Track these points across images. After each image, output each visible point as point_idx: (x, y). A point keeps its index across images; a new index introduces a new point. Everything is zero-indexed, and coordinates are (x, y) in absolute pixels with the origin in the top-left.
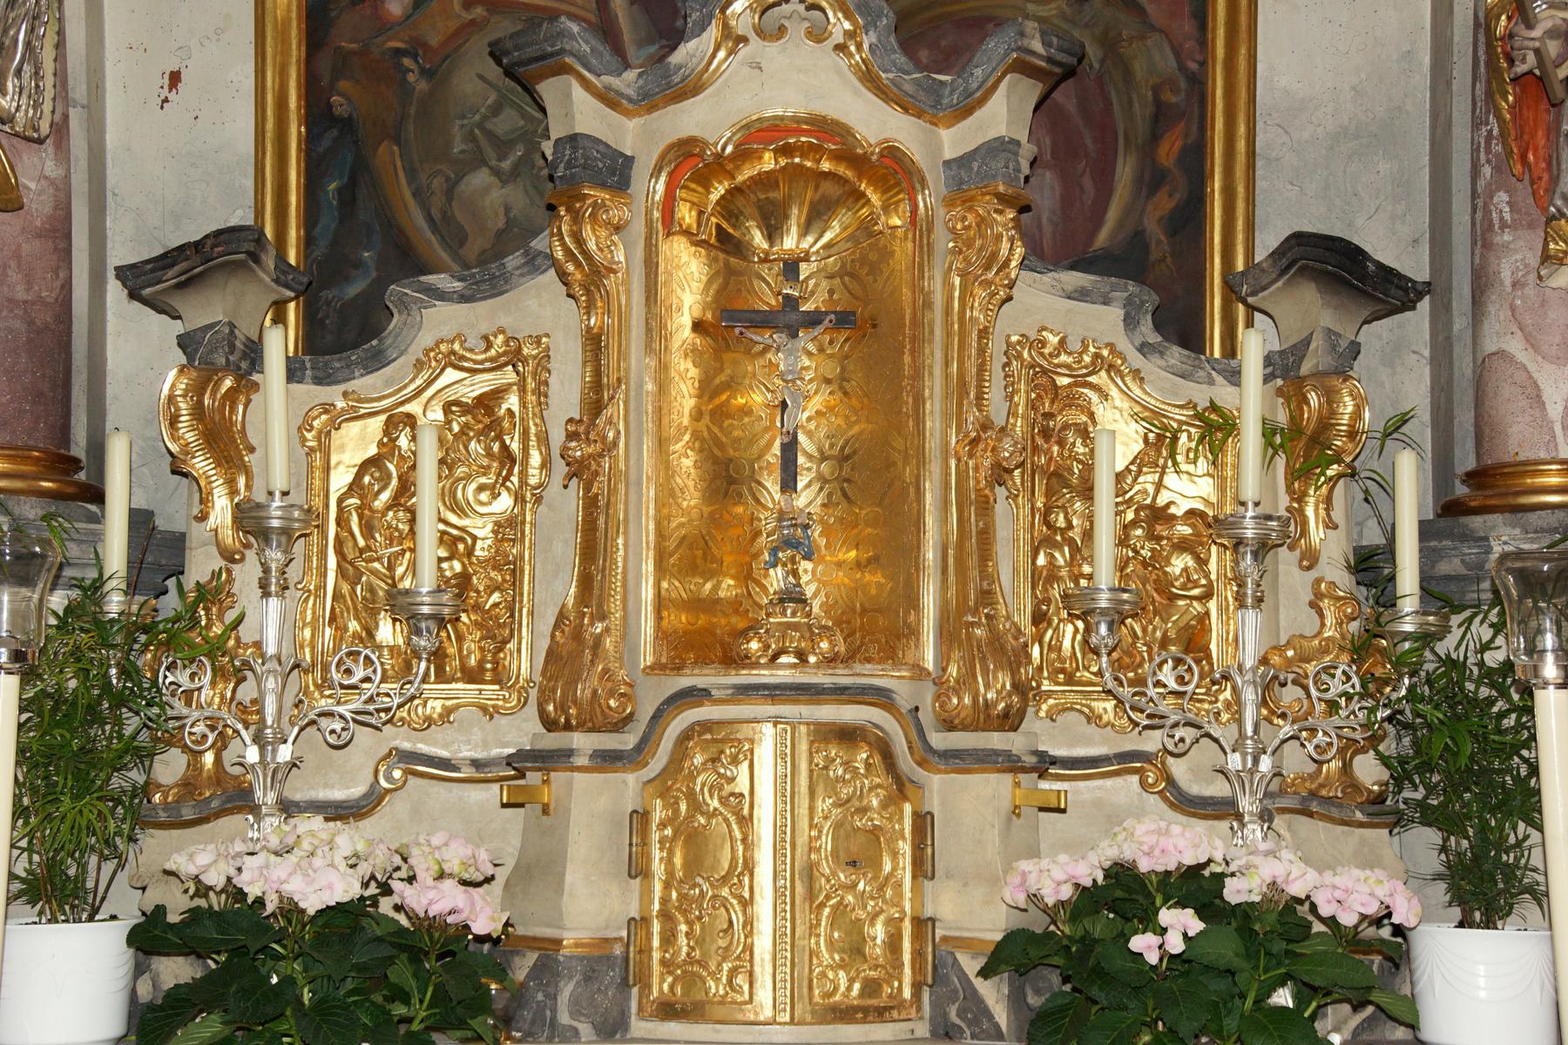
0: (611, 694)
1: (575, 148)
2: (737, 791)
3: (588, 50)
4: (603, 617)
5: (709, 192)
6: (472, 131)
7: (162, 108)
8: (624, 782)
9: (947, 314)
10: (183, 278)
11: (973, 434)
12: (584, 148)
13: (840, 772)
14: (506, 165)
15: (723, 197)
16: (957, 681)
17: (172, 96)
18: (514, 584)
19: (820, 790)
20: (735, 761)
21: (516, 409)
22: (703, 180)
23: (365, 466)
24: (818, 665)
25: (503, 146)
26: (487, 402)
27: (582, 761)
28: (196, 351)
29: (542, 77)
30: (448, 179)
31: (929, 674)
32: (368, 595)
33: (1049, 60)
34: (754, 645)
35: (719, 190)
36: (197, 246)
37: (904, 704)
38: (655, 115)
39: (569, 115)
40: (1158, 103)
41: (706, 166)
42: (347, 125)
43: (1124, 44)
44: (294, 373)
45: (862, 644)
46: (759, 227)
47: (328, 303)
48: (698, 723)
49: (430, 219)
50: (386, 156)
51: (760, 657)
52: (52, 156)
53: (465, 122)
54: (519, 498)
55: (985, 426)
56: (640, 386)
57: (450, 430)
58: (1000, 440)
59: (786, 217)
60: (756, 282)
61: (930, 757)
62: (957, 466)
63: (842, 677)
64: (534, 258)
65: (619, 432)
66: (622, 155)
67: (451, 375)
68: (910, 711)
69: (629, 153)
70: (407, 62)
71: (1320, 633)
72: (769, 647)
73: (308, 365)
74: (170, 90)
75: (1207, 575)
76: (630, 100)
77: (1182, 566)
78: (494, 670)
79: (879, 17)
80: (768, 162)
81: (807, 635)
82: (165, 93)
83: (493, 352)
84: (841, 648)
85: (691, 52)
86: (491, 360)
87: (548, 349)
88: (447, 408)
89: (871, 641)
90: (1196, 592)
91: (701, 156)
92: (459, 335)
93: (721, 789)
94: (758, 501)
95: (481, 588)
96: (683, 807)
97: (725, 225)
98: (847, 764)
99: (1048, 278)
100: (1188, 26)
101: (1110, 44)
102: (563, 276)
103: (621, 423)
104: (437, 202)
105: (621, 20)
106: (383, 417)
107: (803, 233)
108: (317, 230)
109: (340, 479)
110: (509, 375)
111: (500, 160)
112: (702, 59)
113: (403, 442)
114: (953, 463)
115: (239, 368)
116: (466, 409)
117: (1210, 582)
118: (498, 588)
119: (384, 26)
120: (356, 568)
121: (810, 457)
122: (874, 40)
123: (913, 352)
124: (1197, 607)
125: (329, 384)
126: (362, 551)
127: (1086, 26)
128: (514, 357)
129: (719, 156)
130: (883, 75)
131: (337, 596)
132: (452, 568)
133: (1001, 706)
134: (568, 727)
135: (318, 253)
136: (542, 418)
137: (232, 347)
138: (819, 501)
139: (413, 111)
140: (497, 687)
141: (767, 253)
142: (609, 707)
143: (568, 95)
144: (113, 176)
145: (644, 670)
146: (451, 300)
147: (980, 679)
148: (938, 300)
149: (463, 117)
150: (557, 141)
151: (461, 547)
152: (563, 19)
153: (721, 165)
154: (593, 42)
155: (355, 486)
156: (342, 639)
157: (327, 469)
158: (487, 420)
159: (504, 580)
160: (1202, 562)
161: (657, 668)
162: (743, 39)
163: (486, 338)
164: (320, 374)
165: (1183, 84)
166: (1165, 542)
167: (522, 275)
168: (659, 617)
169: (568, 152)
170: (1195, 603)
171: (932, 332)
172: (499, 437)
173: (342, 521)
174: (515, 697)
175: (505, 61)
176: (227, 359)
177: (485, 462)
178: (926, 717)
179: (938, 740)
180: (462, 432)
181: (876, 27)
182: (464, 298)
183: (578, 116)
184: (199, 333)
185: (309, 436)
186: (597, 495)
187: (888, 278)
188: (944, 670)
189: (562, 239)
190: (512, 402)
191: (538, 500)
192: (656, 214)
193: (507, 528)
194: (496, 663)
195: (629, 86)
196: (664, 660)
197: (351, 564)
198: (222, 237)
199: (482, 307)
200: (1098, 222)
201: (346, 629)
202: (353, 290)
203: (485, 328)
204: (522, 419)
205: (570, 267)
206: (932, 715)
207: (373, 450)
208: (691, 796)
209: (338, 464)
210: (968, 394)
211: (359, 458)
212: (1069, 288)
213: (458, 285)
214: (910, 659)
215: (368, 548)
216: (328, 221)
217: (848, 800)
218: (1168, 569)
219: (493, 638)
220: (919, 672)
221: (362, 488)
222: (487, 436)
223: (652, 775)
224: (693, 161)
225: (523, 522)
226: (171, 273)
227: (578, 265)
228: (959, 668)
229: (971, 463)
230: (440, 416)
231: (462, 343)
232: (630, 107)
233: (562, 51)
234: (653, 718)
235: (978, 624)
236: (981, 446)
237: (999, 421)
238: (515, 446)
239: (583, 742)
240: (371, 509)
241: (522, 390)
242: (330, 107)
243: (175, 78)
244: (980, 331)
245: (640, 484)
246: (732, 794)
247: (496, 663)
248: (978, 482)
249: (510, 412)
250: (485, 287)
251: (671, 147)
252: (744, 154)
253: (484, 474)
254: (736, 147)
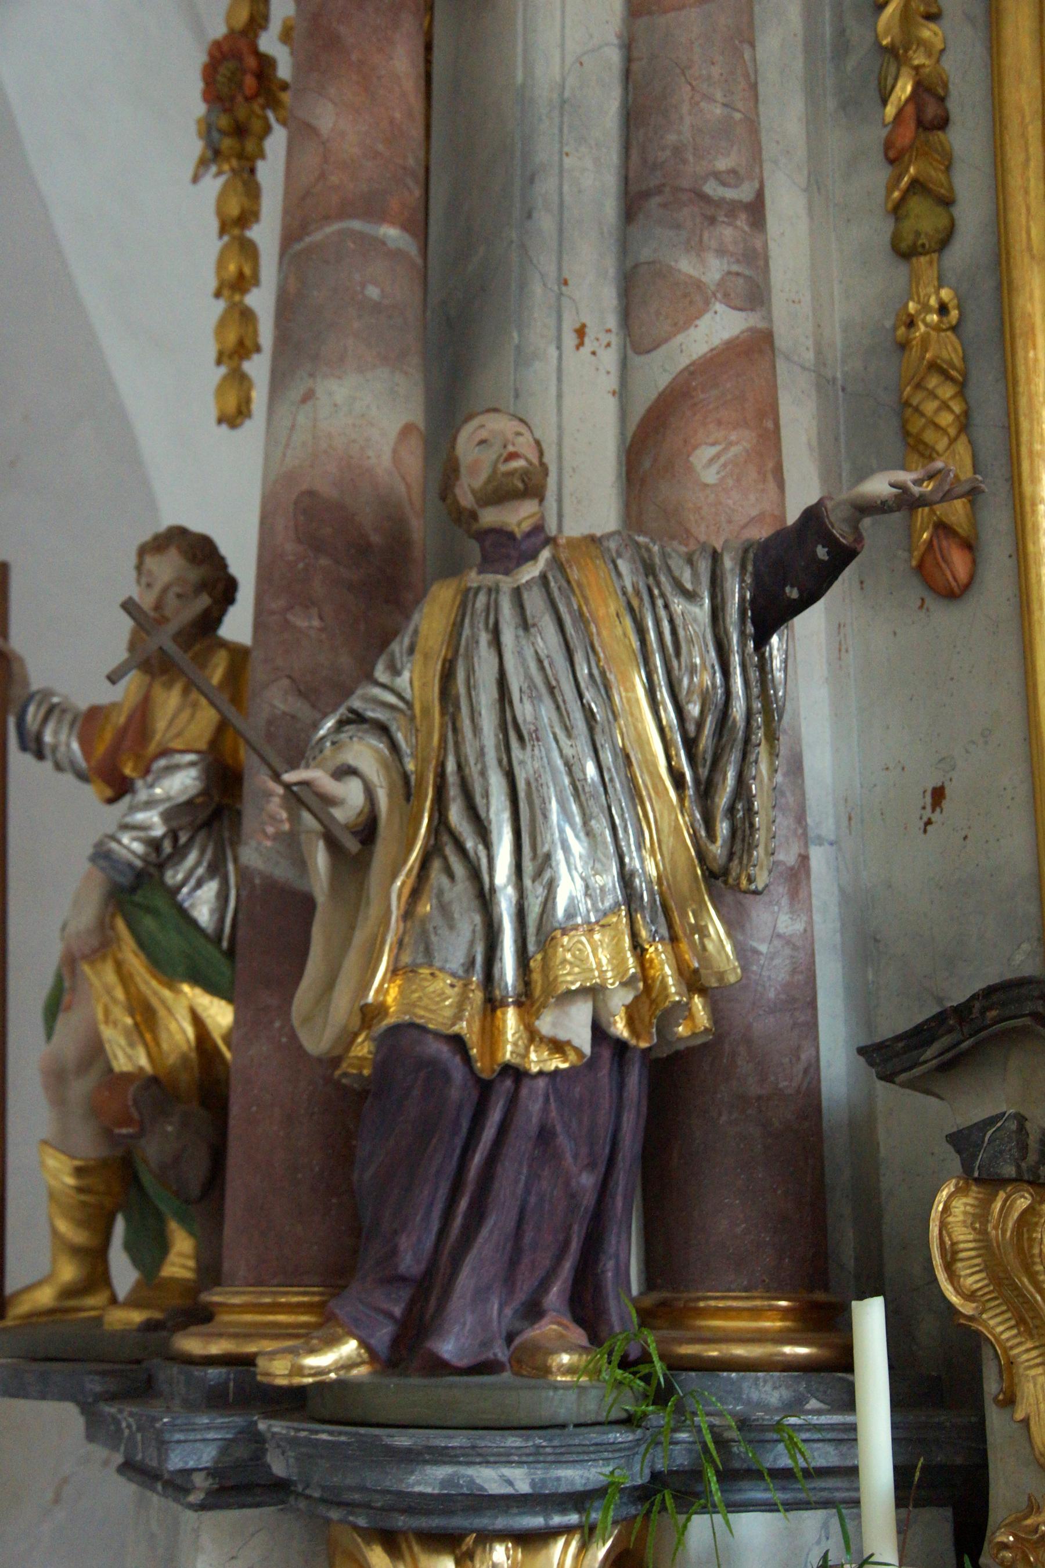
7: (925, 831)
10: (948, 1056)
17: (936, 817)
36: (962, 1012)
52: (786, 909)
74: (933, 811)
176: (1018, 1167)
198: (995, 998)
226: (929, 1053)
243: (938, 795)
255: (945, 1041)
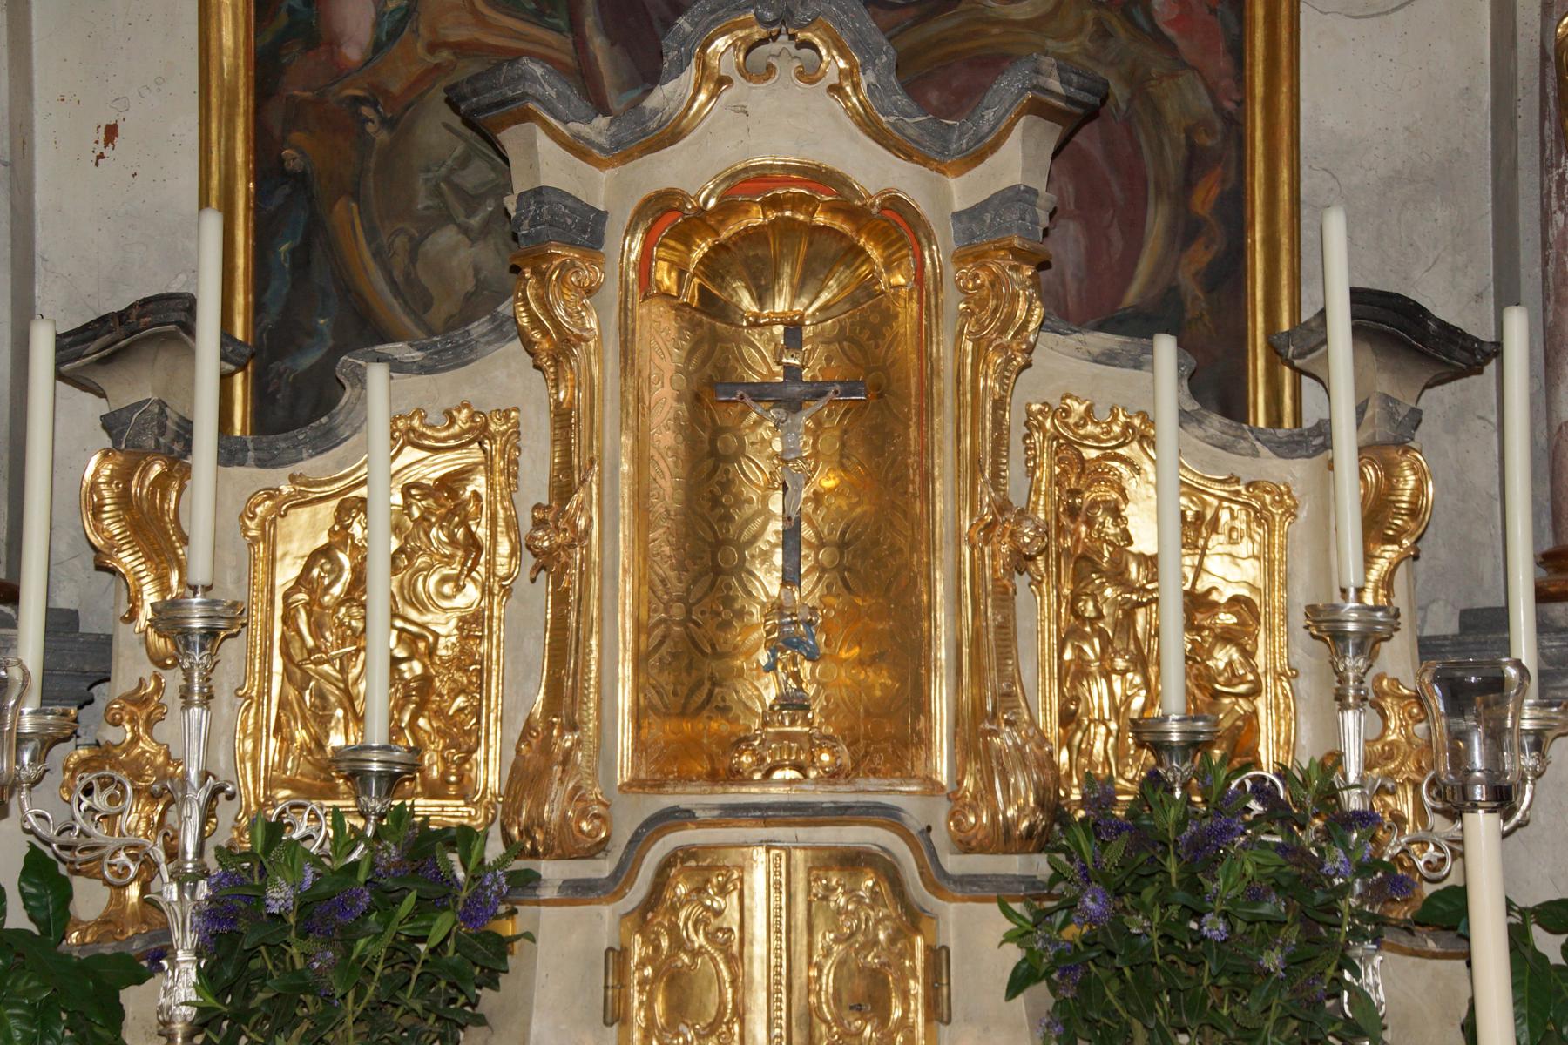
0: (583, 814)
1: (540, 203)
2: (725, 925)
3: (553, 94)
4: (573, 727)
5: (691, 251)
6: (437, 185)
7: (97, 164)
8: (599, 915)
9: (959, 382)
10: (106, 352)
11: (989, 518)
12: (550, 203)
13: (842, 902)
14: (475, 221)
15: (705, 255)
16: (974, 797)
17: (108, 152)
18: (480, 686)
19: (820, 922)
20: (723, 891)
21: (483, 491)
22: (684, 236)
23: (313, 558)
24: (817, 780)
25: (471, 201)
26: (450, 484)
27: (548, 893)
28: (122, 433)
29: (503, 125)
30: (411, 238)
31: (942, 788)
32: (318, 702)
33: (1069, 100)
34: (746, 759)
35: (701, 250)
36: (122, 316)
37: (915, 824)
38: (630, 165)
39: (533, 167)
40: (1191, 146)
41: (685, 221)
42: (301, 181)
43: (1153, 82)
44: (229, 453)
45: (867, 753)
46: (748, 288)
47: (280, 376)
48: (681, 848)
49: (392, 283)
50: (344, 214)
51: (752, 773)
53: (430, 175)
54: (486, 591)
55: (1003, 507)
56: (616, 466)
57: (410, 515)
58: (1018, 523)
59: (777, 276)
60: (745, 349)
61: (944, 883)
62: (972, 554)
63: (844, 795)
64: (501, 325)
65: (591, 520)
66: (593, 209)
67: (411, 454)
68: (921, 832)
69: (602, 208)
70: (366, 111)
71: (1383, 735)
72: (763, 759)
73: (250, 446)
74: (106, 146)
75: (1254, 670)
76: (601, 148)
77: (1226, 660)
78: (459, 782)
79: (878, 54)
80: (757, 218)
81: (807, 746)
82: (100, 148)
83: (456, 429)
84: (845, 759)
85: (668, 95)
86: (455, 437)
87: (517, 424)
88: (406, 491)
89: (876, 751)
90: (1242, 688)
91: (680, 210)
92: (418, 411)
93: (706, 925)
94: (749, 594)
95: (445, 692)
96: (665, 943)
97: (709, 286)
98: (851, 893)
99: (1072, 340)
100: (1224, 63)
101: (1138, 82)
102: (529, 346)
103: (595, 509)
104: (399, 263)
105: (600, 58)
106: (335, 503)
107: (795, 296)
108: (268, 295)
109: (287, 573)
110: (474, 454)
111: (468, 216)
112: (681, 102)
113: (357, 530)
114: (967, 551)
115: (172, 451)
116: (426, 491)
117: (1257, 676)
118: (462, 691)
119: (341, 73)
120: (304, 672)
121: (810, 545)
122: (873, 80)
123: (920, 425)
124: (1244, 706)
125: (274, 467)
126: (310, 652)
127: (1112, 64)
128: (480, 434)
129: (701, 210)
130: (883, 119)
131: (283, 703)
132: (411, 669)
133: (1025, 824)
134: (534, 854)
135: (269, 320)
136: (512, 501)
137: (162, 428)
138: (817, 593)
139: (372, 163)
140: (461, 802)
141: (757, 317)
142: (581, 831)
143: (533, 144)
144: (43, 240)
145: (621, 788)
146: (410, 372)
147: (999, 794)
148: (948, 367)
149: (428, 170)
150: (521, 195)
151: (422, 645)
152: (525, 60)
153: (703, 221)
154: (561, 87)
155: (303, 580)
156: (288, 751)
157: (272, 562)
158: (451, 504)
159: (470, 682)
160: (1248, 655)
161: (636, 785)
162: (723, 81)
163: (448, 413)
164: (263, 455)
165: (1219, 125)
166: (1207, 633)
167: (489, 343)
168: (637, 727)
169: (532, 208)
170: (1241, 701)
171: (941, 403)
172: (464, 523)
173: (289, 619)
174: (482, 813)
175: (463, 107)
176: (157, 441)
177: (447, 551)
178: (940, 838)
179: (954, 863)
180: (423, 518)
181: (874, 66)
182: (424, 369)
183: (543, 168)
184: (125, 413)
185: (251, 524)
186: (567, 589)
187: (890, 345)
188: (960, 783)
189: (526, 304)
190: (479, 483)
191: (507, 592)
192: (632, 275)
193: (472, 623)
194: (461, 777)
195: (600, 133)
196: (643, 775)
197: (299, 666)
198: (151, 306)
199: (444, 379)
200: (1128, 277)
201: (293, 740)
202: (307, 361)
203: (447, 402)
204: (490, 503)
205: (537, 336)
206: (946, 836)
207: (323, 540)
208: (673, 931)
209: (285, 555)
210: (983, 473)
211: (308, 550)
212: (1096, 351)
213: (417, 355)
214: (920, 770)
215: (317, 649)
216: (280, 286)
217: (852, 934)
218: (1210, 663)
219: (458, 747)
220: (931, 786)
221: (311, 582)
222: (450, 521)
223: (631, 907)
224: (671, 217)
225: (491, 618)
226: (92, 347)
227: (545, 333)
228: (976, 782)
229: (987, 550)
230: (397, 499)
231: (422, 419)
232: (603, 156)
233: (524, 96)
234: (630, 842)
235: (996, 733)
236: (999, 530)
237: (1018, 501)
238: (482, 532)
239: (552, 871)
240: (321, 605)
241: (490, 471)
242: (281, 161)
243: (111, 132)
244: (995, 402)
245: (615, 577)
246: (720, 929)
247: (461, 777)
248: (995, 571)
249: (476, 495)
250: (448, 356)
251: (648, 201)
252: (728, 208)
253: (448, 564)
254: (719, 200)
255: (107, 338)
